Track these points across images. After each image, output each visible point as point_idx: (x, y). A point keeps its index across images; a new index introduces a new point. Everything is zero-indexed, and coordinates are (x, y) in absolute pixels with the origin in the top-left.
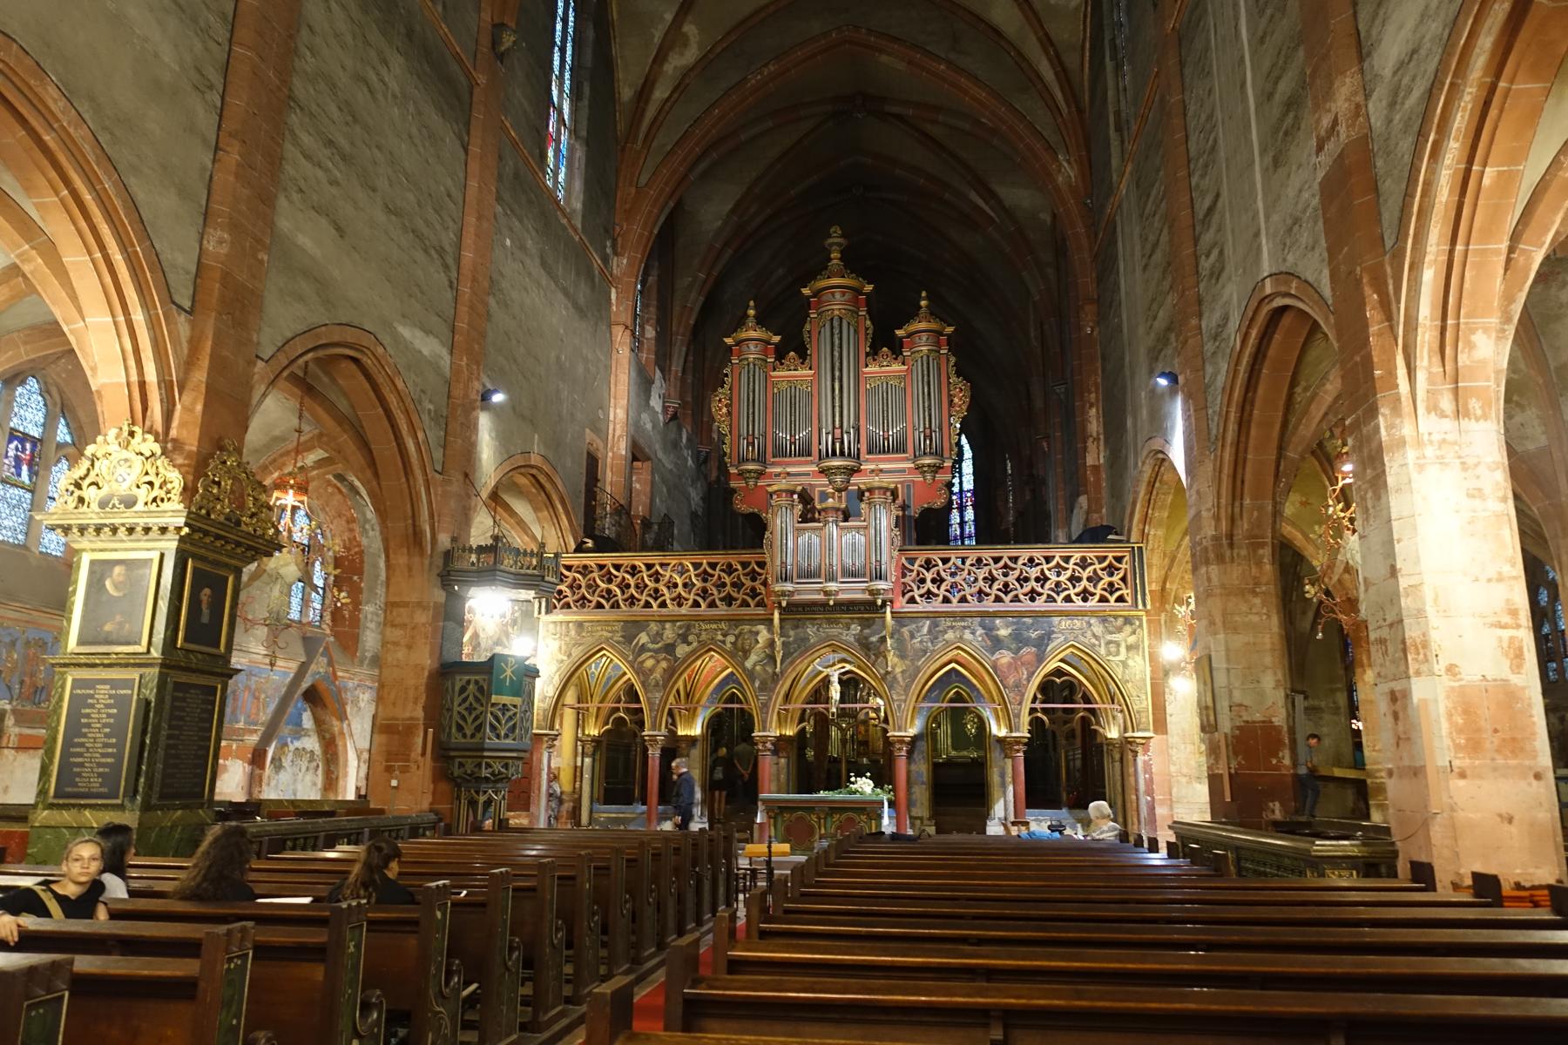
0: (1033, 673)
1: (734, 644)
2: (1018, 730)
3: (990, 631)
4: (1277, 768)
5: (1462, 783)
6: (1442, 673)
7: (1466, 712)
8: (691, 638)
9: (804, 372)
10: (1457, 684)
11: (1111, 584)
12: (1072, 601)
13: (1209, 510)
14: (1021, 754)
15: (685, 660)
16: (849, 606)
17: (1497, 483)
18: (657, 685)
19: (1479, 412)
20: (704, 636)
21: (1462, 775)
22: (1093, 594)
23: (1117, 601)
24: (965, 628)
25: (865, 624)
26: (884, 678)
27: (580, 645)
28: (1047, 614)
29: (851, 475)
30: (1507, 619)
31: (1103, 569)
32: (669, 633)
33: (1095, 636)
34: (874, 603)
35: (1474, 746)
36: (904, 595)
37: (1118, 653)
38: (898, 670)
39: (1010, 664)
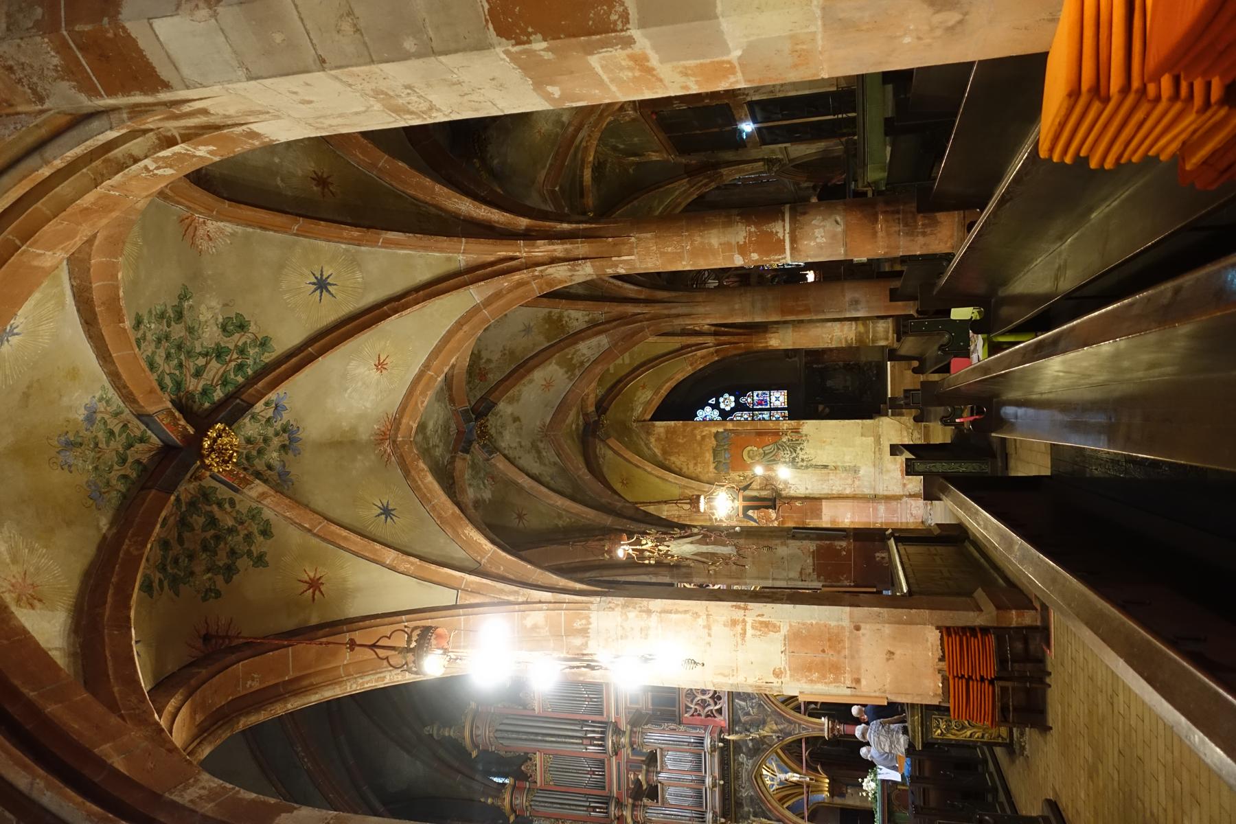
4: (849, 551)
5: (863, 682)
6: (780, 681)
7: (809, 669)
9: (538, 758)
10: (788, 672)
13: (651, 578)
16: (724, 764)
17: (637, 616)
19: (584, 622)
21: (858, 681)
29: (620, 730)
30: (739, 628)
34: (721, 748)
35: (836, 669)
36: (715, 717)
38: (775, 727)
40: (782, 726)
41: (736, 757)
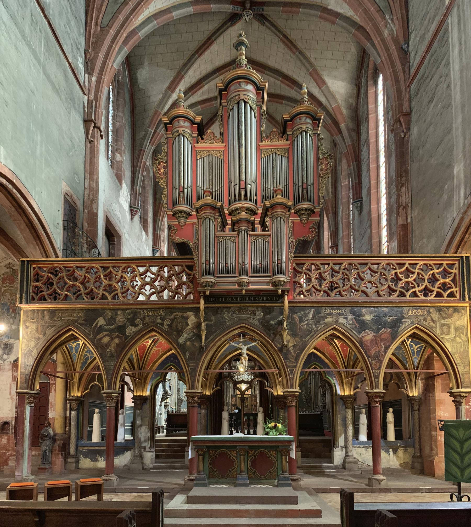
0: (389, 347)
1: (170, 326)
2: (377, 387)
3: (357, 316)
8: (137, 321)
11: (444, 284)
12: (417, 296)
14: (378, 405)
15: (132, 338)
18: (112, 355)
20: (147, 320)
22: (432, 291)
23: (448, 296)
24: (339, 314)
25: (267, 311)
26: (281, 350)
27: (53, 326)
28: (398, 305)
31: (438, 273)
32: (121, 318)
33: (433, 320)
37: (449, 333)
39: (372, 341)
40: (292, 351)
41: (260, 309)
